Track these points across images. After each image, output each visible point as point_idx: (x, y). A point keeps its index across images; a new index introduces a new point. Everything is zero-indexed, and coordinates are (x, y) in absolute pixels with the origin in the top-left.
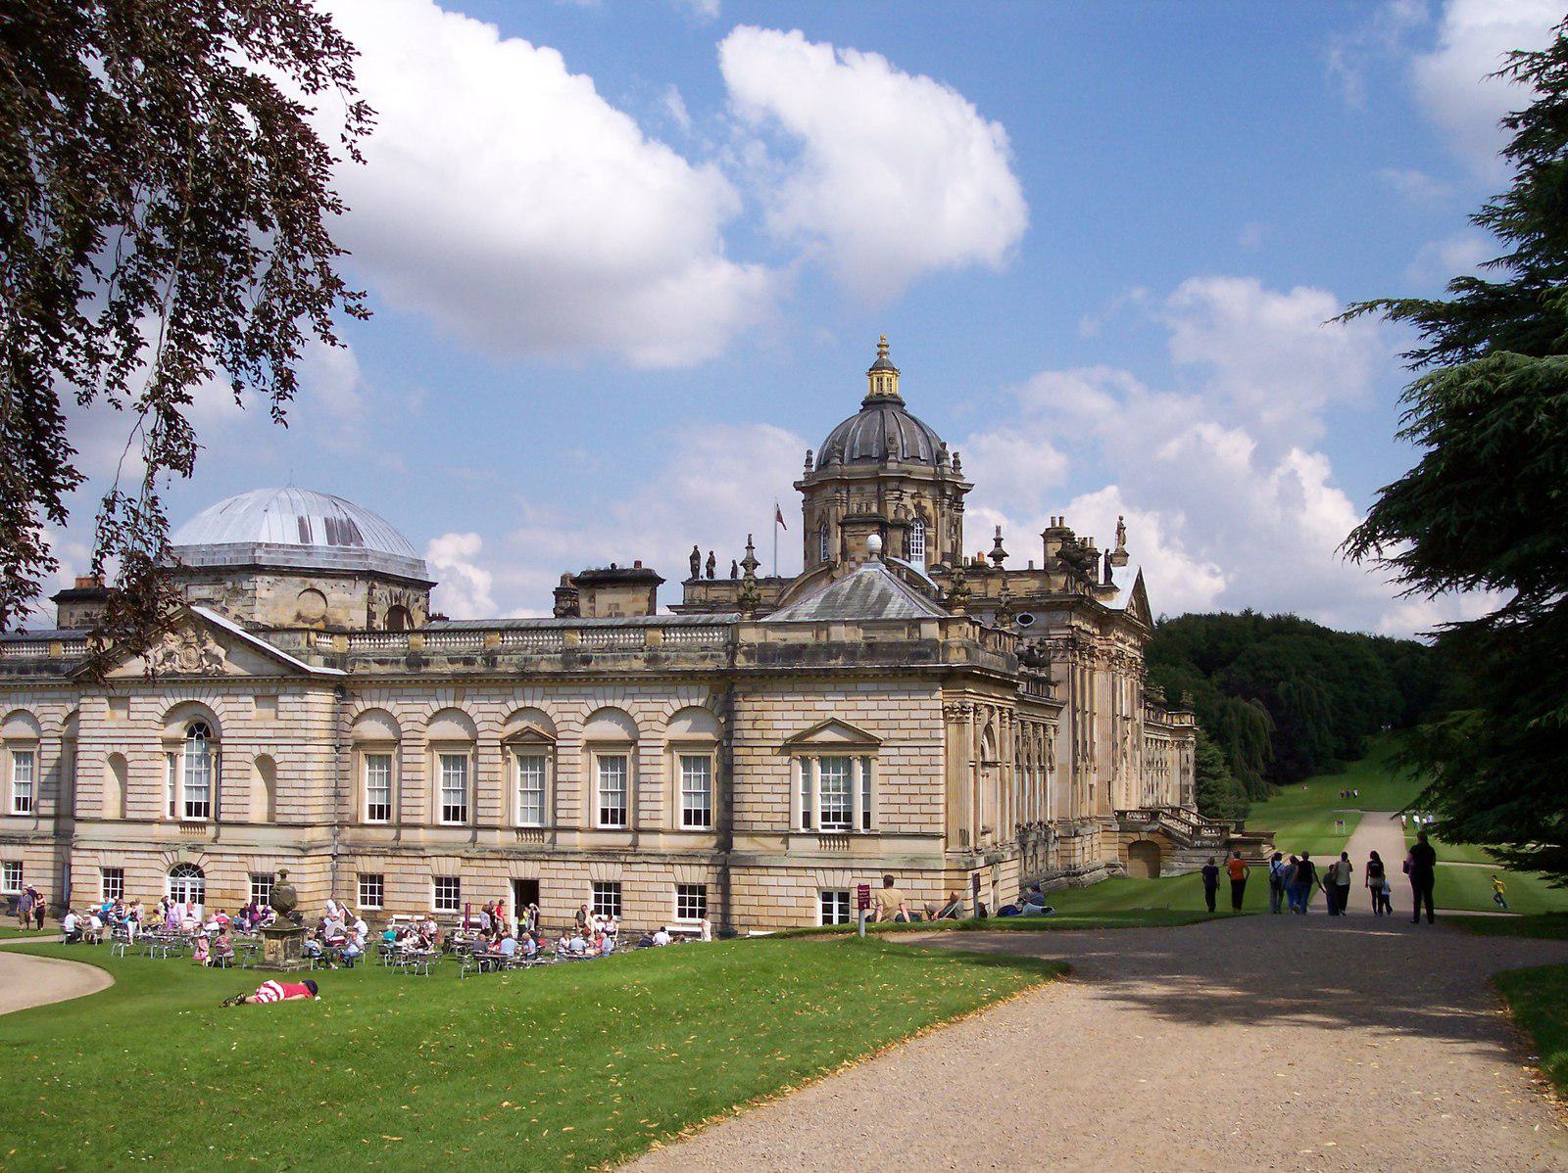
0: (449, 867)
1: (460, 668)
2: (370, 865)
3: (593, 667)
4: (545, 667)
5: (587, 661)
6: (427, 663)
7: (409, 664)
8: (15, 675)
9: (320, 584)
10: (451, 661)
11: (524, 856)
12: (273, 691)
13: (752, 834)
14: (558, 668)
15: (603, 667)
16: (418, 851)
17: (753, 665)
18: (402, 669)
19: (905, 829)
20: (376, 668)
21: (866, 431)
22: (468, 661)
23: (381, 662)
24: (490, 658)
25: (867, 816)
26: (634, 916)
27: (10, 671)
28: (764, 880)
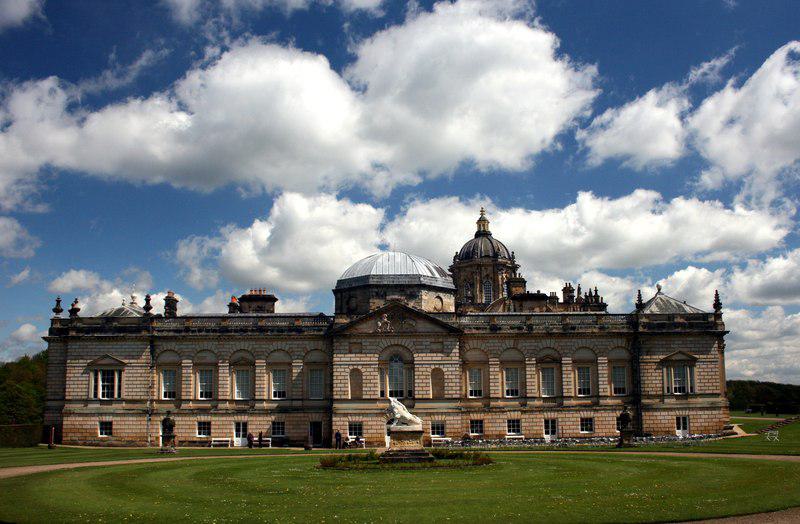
0: (515, 415)
1: (516, 331)
2: (475, 416)
3: (576, 331)
4: (555, 331)
5: (574, 328)
6: (500, 329)
7: (491, 329)
8: (276, 333)
9: (441, 295)
10: (512, 328)
11: (550, 409)
12: (441, 340)
13: (649, 397)
14: (561, 331)
15: (581, 331)
16: (501, 410)
17: (645, 330)
18: (488, 331)
19: (707, 392)
20: (474, 331)
21: (485, 246)
22: (520, 328)
23: (477, 329)
24: (530, 327)
25: (691, 388)
26: (599, 431)
27: (272, 331)
28: (655, 414)
